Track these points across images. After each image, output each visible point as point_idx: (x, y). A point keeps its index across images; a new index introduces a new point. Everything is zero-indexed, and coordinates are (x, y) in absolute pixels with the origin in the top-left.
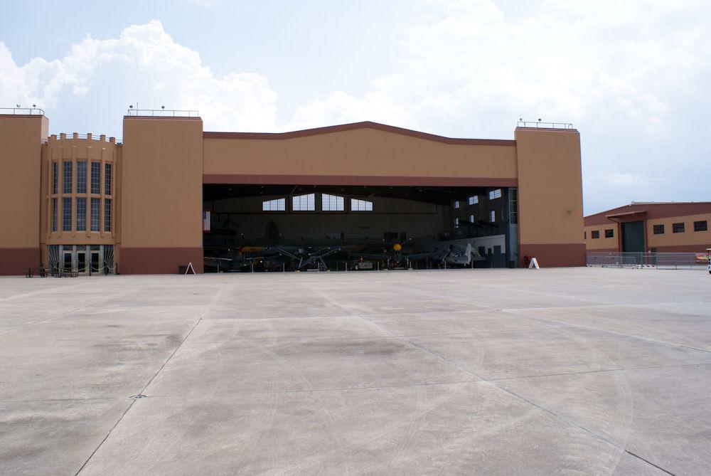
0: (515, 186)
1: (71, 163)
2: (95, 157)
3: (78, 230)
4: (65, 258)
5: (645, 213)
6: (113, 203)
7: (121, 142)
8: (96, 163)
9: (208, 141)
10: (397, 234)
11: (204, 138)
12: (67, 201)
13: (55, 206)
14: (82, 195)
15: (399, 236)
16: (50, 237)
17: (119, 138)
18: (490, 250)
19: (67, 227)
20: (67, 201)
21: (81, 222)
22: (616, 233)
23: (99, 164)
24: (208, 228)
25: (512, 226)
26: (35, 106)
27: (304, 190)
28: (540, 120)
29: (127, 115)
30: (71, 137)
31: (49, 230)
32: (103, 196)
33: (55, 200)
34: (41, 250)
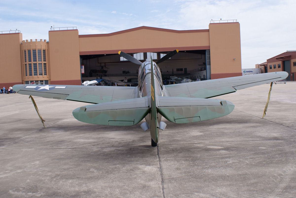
0: (208, 49)
1: (30, 50)
2: (38, 47)
3: (34, 75)
5: (290, 56)
6: (47, 65)
8: (39, 50)
10: (182, 69)
11: (79, 37)
12: (30, 65)
13: (26, 67)
14: (35, 62)
16: (25, 78)
17: (48, 40)
19: (31, 75)
20: (30, 65)
21: (36, 72)
22: (281, 66)
24: (83, 72)
25: (208, 66)
26: (17, 29)
27: (137, 51)
31: (25, 76)
32: (43, 62)
33: (26, 65)
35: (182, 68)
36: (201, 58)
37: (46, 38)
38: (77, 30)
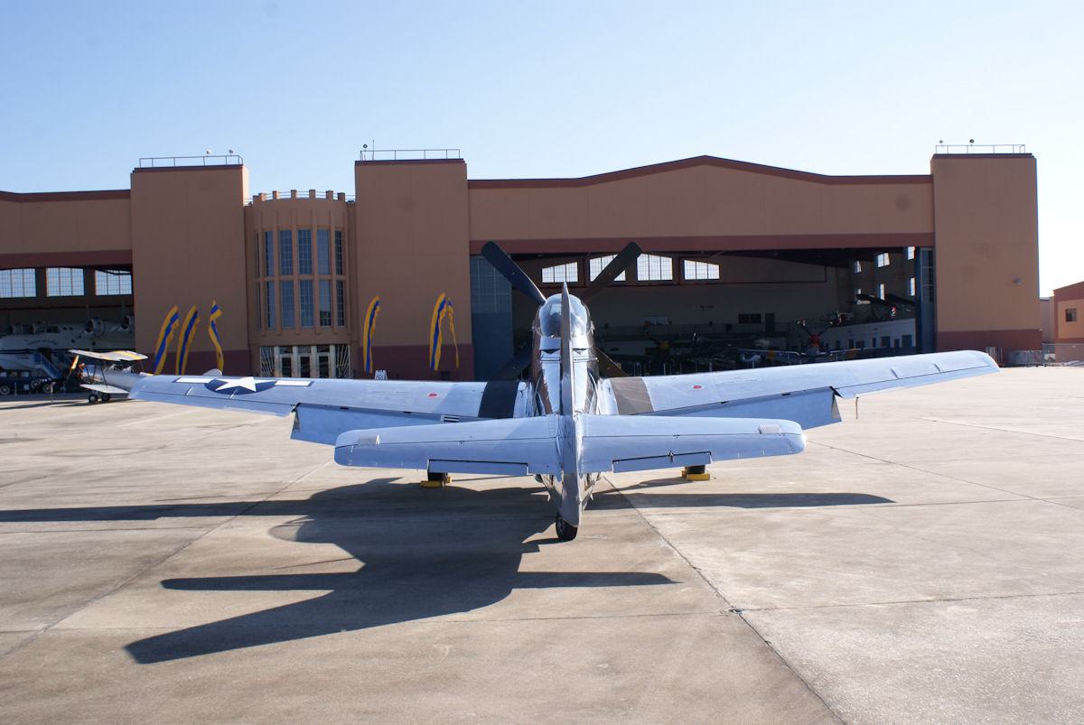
1: (290, 232)
4: (283, 362)
7: (353, 198)
9: (475, 192)
10: (759, 315)
11: (469, 188)
14: (306, 277)
15: (763, 320)
16: (264, 336)
17: (351, 195)
18: (897, 341)
23: (309, 231)
28: (972, 141)
29: (359, 159)
30: (289, 196)
34: (250, 351)
35: (758, 312)
36: (824, 280)
37: (347, 187)
38: (461, 161)
